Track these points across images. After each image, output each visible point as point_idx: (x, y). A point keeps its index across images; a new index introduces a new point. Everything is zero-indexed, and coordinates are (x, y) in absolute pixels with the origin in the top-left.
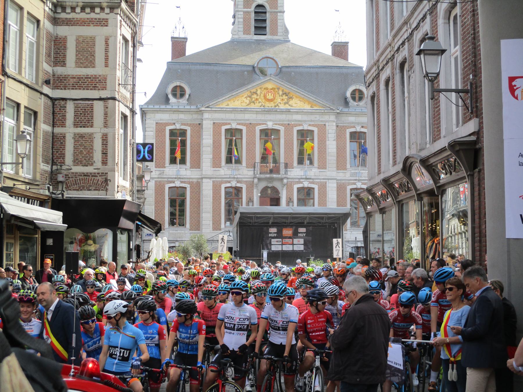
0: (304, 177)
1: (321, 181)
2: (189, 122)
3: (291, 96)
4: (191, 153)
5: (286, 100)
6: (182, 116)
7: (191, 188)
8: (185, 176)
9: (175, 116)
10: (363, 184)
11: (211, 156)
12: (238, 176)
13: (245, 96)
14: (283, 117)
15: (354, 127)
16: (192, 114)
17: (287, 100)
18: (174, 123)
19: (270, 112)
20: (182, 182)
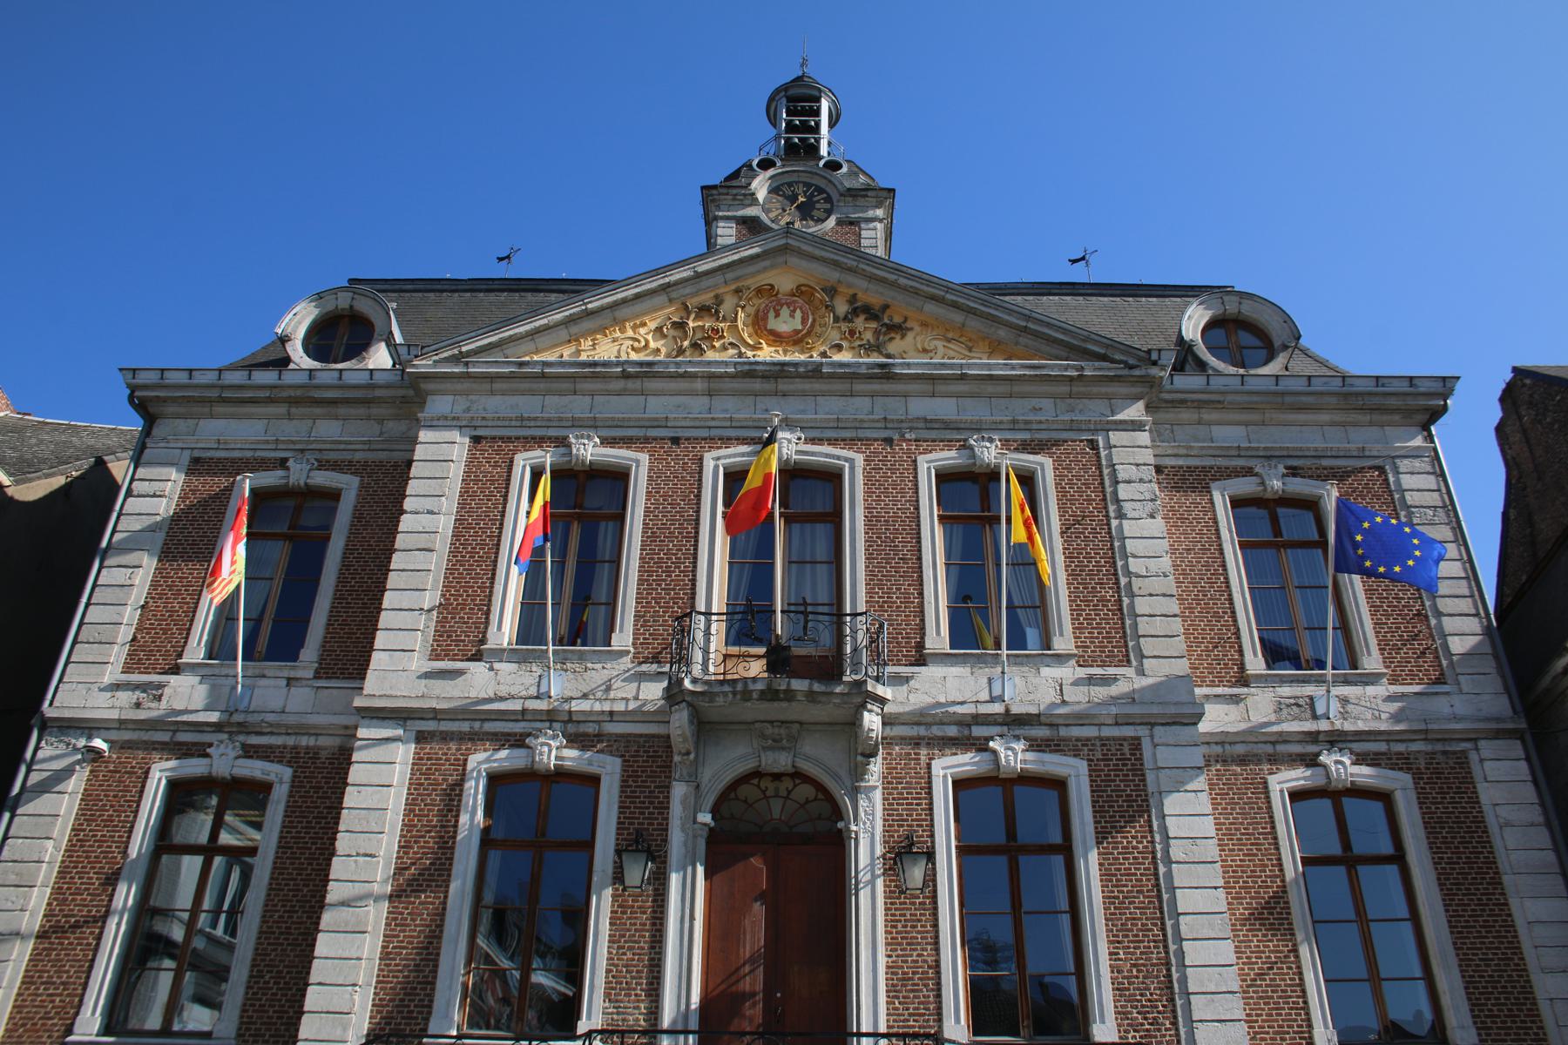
0: (998, 708)
1: (1107, 732)
2: (358, 456)
3: (897, 319)
4: (339, 597)
5: (868, 336)
6: (328, 430)
7: (296, 783)
8: (270, 718)
9: (293, 429)
10: (1360, 759)
11: (431, 598)
12: (576, 706)
13: (652, 325)
14: (859, 407)
15: (1249, 472)
16: (381, 421)
17: (877, 333)
18: (282, 463)
19: (783, 386)
20: (249, 752)
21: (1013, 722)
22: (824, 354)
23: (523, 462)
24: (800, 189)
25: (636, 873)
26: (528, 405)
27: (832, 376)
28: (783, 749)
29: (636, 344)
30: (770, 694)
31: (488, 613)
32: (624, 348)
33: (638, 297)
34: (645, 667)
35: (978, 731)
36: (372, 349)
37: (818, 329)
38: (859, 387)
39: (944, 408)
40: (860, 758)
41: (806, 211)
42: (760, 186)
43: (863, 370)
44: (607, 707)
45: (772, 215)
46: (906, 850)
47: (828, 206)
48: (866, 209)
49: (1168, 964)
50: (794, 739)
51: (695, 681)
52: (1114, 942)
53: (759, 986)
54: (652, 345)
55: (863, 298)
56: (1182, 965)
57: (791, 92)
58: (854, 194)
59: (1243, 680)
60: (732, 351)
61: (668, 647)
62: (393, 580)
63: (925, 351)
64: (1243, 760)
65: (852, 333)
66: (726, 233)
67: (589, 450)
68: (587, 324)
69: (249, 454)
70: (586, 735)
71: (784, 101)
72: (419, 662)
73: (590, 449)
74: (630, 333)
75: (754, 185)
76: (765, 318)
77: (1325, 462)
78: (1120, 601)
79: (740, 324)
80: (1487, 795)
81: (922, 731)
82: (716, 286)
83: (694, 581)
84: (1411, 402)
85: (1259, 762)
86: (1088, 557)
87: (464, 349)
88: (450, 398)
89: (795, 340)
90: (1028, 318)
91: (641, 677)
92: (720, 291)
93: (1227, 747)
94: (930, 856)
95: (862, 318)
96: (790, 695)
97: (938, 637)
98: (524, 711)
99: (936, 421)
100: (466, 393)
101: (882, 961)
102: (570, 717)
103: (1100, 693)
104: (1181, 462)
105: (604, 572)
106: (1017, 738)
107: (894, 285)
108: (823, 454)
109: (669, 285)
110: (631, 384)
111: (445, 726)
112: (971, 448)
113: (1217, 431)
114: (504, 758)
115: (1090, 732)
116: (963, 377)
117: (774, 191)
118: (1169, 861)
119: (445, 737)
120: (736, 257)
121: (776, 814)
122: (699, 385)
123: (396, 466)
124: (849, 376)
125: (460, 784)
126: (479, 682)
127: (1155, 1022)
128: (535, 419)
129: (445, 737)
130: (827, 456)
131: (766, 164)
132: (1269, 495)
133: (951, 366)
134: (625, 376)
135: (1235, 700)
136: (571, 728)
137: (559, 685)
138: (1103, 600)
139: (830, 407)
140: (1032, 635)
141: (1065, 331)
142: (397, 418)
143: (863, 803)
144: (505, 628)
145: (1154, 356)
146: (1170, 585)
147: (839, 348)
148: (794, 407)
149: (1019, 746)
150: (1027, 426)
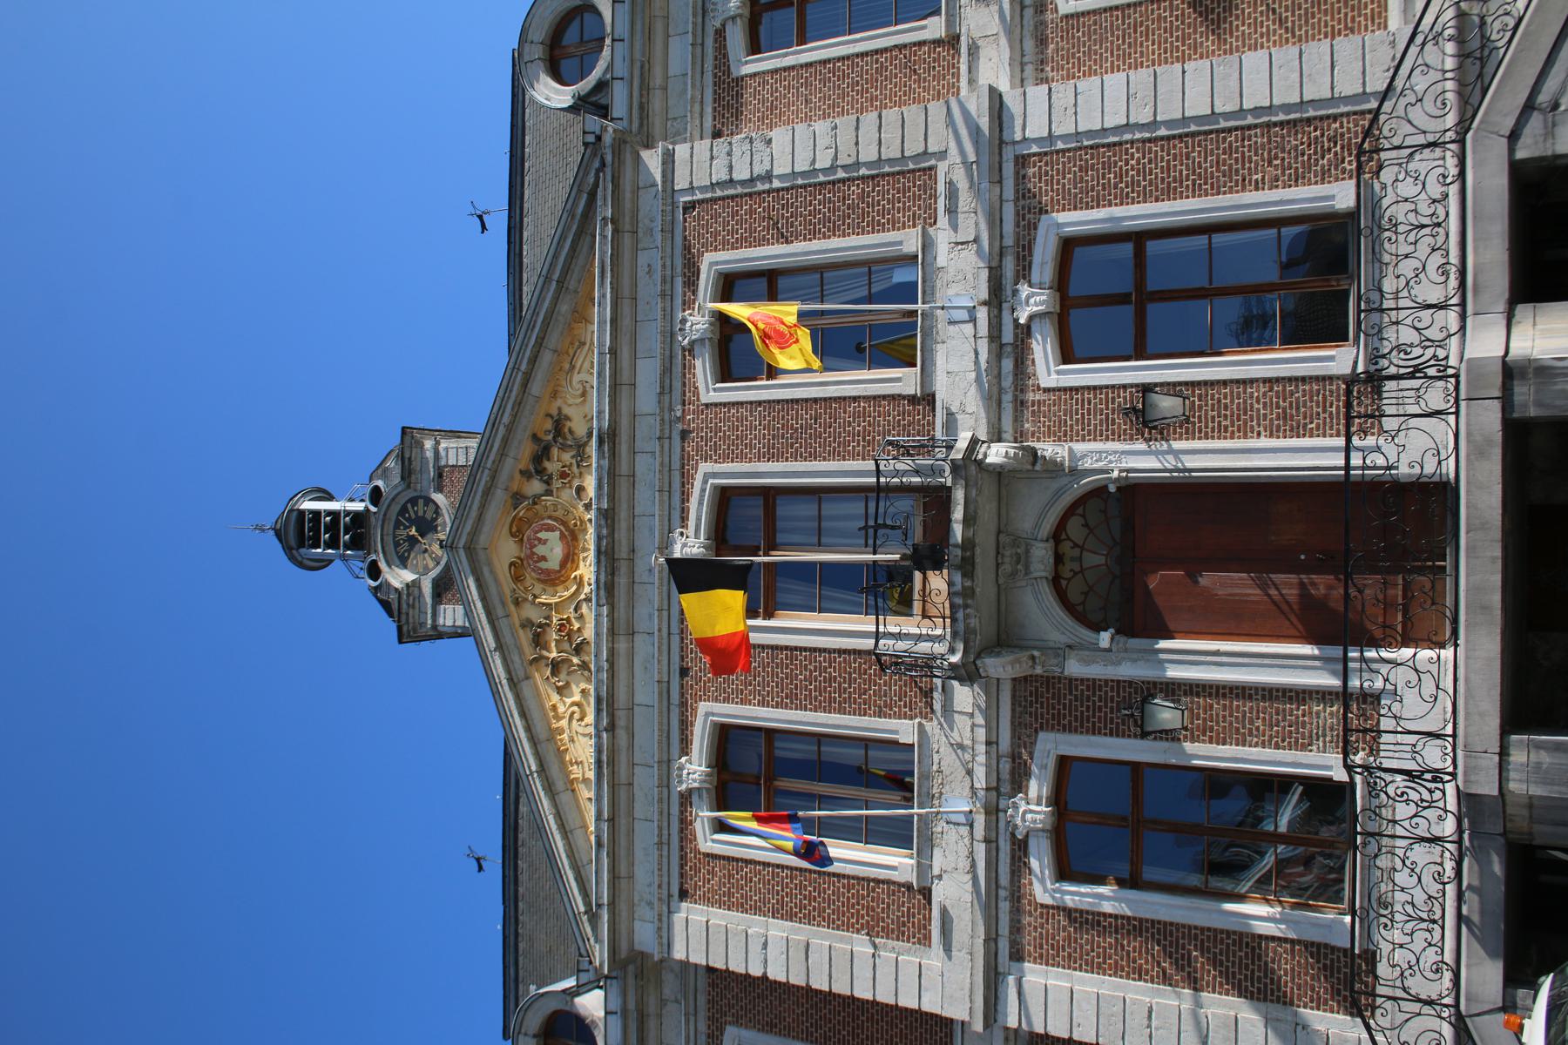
0: (982, 314)
2: (702, 1027)
3: (549, 425)
5: (567, 457)
11: (861, 945)
12: (981, 782)
13: (555, 698)
15: (720, 34)
16: (663, 1003)
17: (564, 448)
19: (622, 552)
21: (998, 297)
22: (588, 507)
23: (709, 842)
24: (402, 532)
25: (1166, 714)
26: (645, 836)
27: (612, 497)
28: (1027, 551)
29: (577, 716)
30: (967, 566)
31: (878, 881)
32: (580, 730)
34: (937, 706)
35: (1008, 336)
36: (582, 1012)
37: (560, 513)
38: (624, 468)
39: (647, 373)
40: (1038, 467)
41: (427, 527)
42: (399, 577)
43: (606, 463)
44: (982, 748)
45: (431, 564)
46: (1139, 413)
47: (421, 502)
48: (424, 460)
49: (1269, 125)
50: (1016, 541)
51: (952, 651)
52: (1243, 185)
53: (1293, 578)
54: (577, 698)
55: (525, 462)
56: (1270, 109)
57: (293, 542)
58: (407, 474)
59: (952, 41)
60: (584, 609)
61: (914, 680)
62: (841, 988)
63: (584, 394)
64: (1042, 42)
65: (563, 475)
66: (451, 615)
67: (695, 768)
68: (554, 771)
70: (1013, 772)
71: (303, 551)
72: (933, 958)
73: (694, 767)
74: (564, 723)
75: (396, 584)
76: (548, 572)
78: (863, 178)
79: (553, 600)
81: (1008, 398)
82: (511, 627)
83: (841, 652)
85: (1043, 23)
86: (813, 213)
87: (582, 909)
88: (637, 924)
89: (572, 537)
90: (548, 279)
91: (948, 709)
93: (1026, 59)
94: (1146, 389)
95: (547, 464)
96: (968, 544)
97: (905, 380)
98: (987, 841)
99: (662, 382)
100: (632, 907)
101: (1265, 442)
102: (994, 789)
103: (965, 200)
104: (709, 110)
105: (831, 752)
106: (1015, 292)
107: (510, 429)
108: (699, 508)
109: (510, 680)
110: (621, 722)
111: (1004, 929)
112: (692, 343)
113: (675, 68)
114: (1040, 862)
115: (1009, 211)
116: (613, 352)
117: (404, 562)
118: (1154, 124)
119: (1016, 928)
120: (479, 605)
121: (1100, 560)
122: (622, 645)
123: (713, 985)
124: (610, 479)
125: (1068, 912)
126: (955, 891)
127: (1333, 140)
128: (660, 828)
129: (1016, 928)
130: (700, 503)
131: (374, 571)
132: (746, 12)
133: (601, 364)
134: (611, 728)
135: (974, 50)
136: (1006, 788)
137: (957, 801)
138: (862, 197)
139: (647, 500)
140: (900, 276)
141: (563, 238)
142: (659, 984)
143: (1088, 464)
144: (895, 862)
145: (591, 138)
146: (845, 122)
147: (580, 490)
148: (647, 541)
149: (1025, 290)
150: (668, 281)
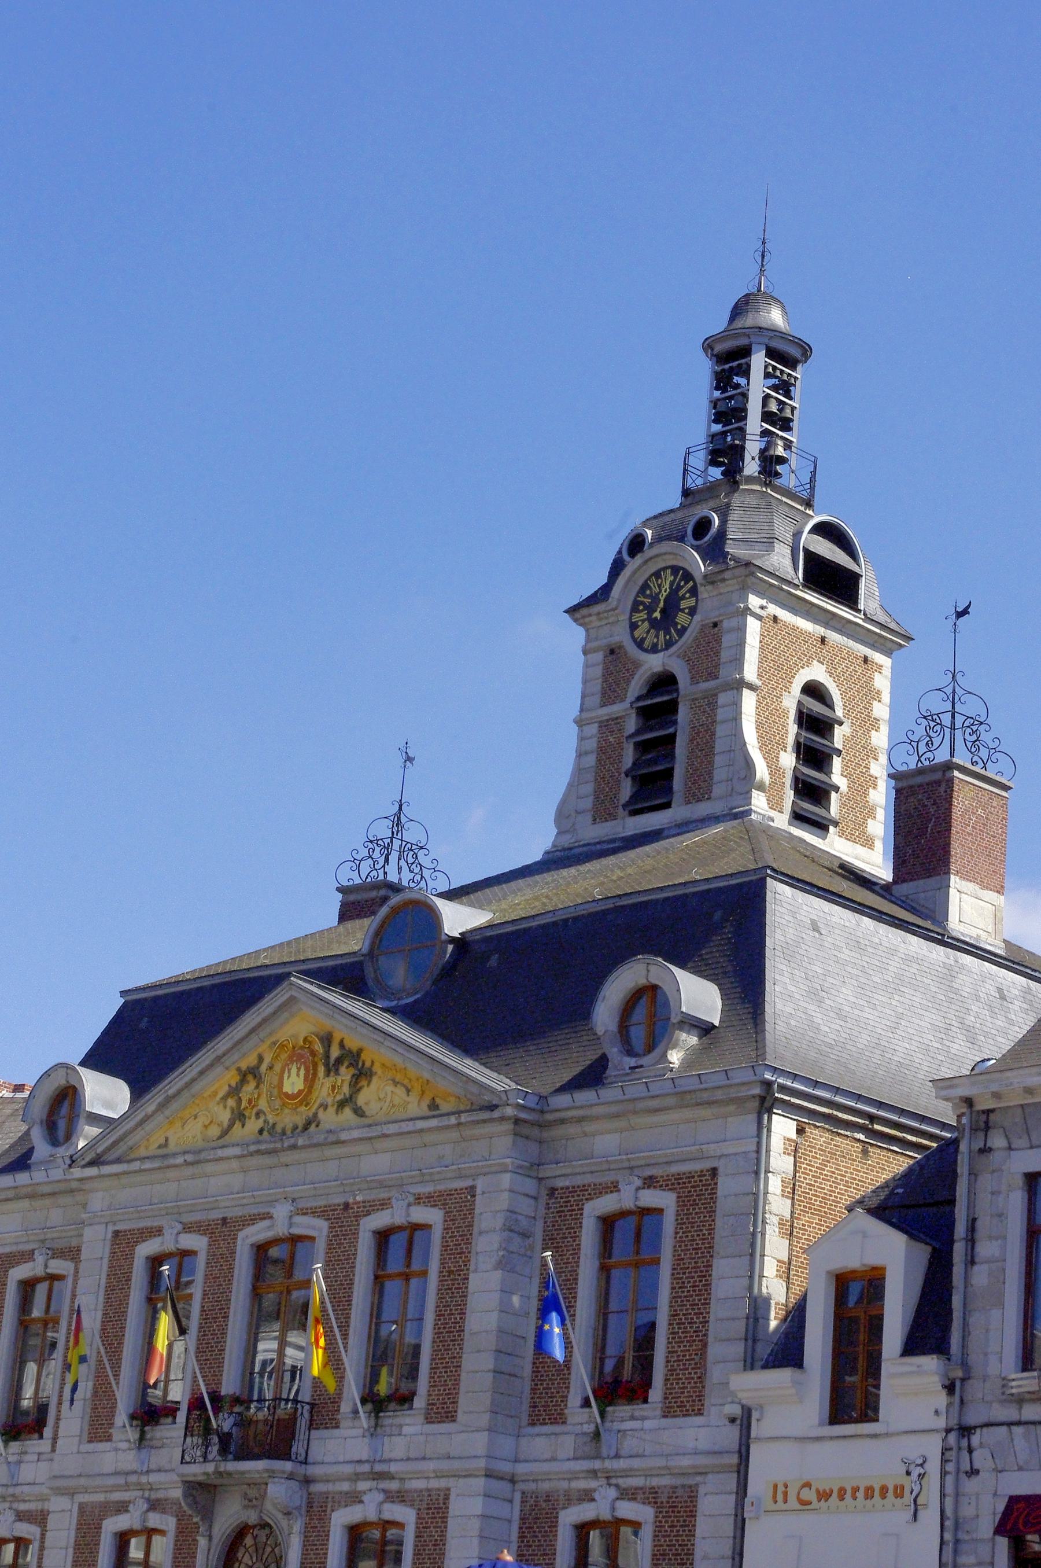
1: (434, 1484)
18: (33, 1251)
33: (202, 1073)
69: (14, 1248)
77: (674, 1169)
80: (702, 1526)
84: (733, 1093)
92: (260, 1050)
136: (154, 1496)
